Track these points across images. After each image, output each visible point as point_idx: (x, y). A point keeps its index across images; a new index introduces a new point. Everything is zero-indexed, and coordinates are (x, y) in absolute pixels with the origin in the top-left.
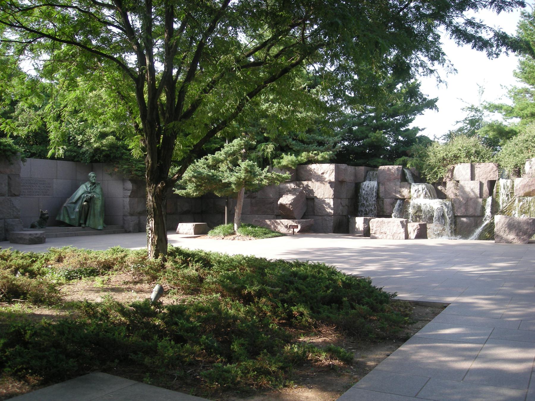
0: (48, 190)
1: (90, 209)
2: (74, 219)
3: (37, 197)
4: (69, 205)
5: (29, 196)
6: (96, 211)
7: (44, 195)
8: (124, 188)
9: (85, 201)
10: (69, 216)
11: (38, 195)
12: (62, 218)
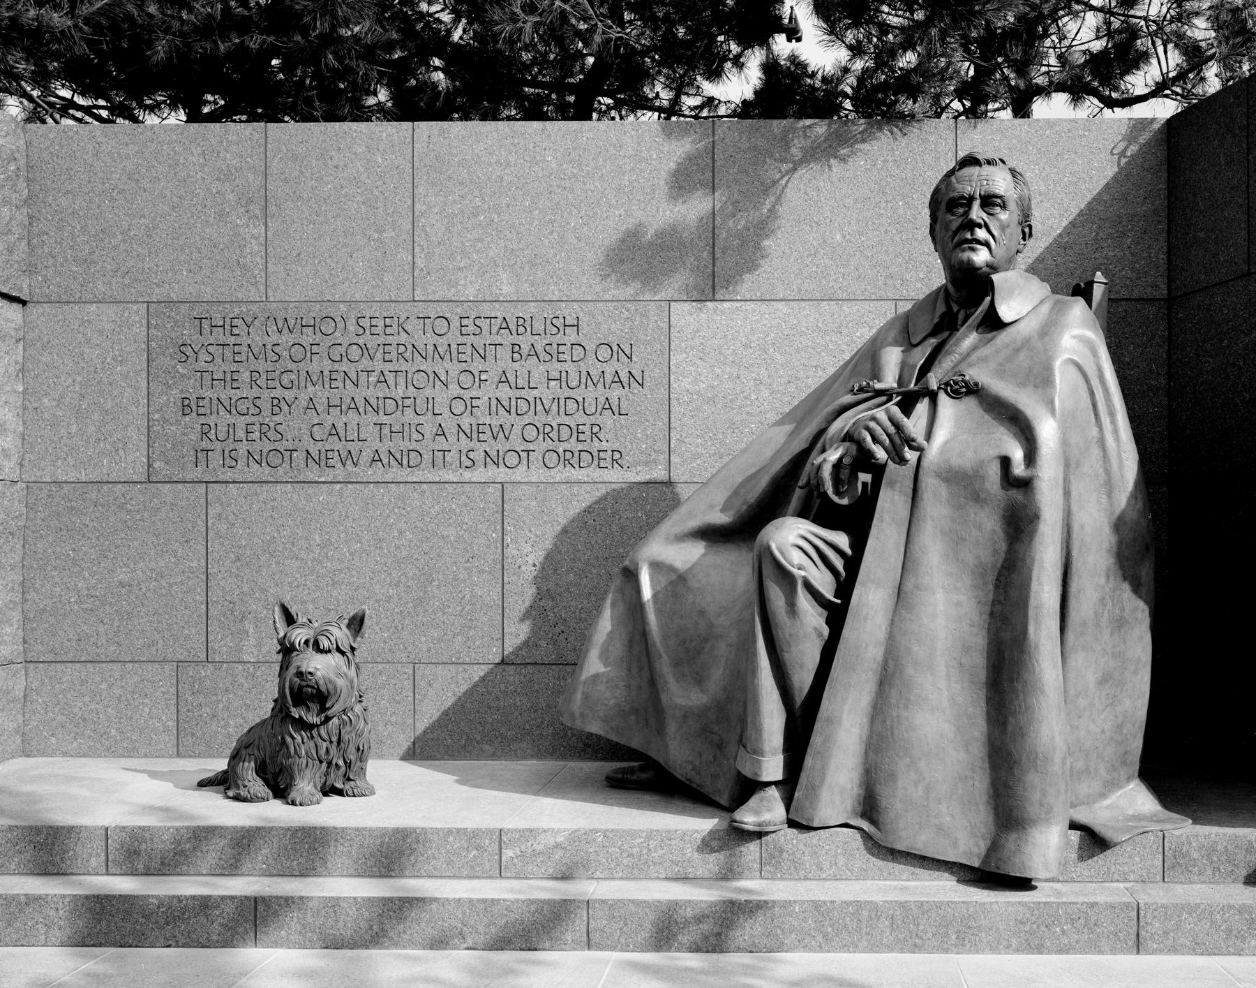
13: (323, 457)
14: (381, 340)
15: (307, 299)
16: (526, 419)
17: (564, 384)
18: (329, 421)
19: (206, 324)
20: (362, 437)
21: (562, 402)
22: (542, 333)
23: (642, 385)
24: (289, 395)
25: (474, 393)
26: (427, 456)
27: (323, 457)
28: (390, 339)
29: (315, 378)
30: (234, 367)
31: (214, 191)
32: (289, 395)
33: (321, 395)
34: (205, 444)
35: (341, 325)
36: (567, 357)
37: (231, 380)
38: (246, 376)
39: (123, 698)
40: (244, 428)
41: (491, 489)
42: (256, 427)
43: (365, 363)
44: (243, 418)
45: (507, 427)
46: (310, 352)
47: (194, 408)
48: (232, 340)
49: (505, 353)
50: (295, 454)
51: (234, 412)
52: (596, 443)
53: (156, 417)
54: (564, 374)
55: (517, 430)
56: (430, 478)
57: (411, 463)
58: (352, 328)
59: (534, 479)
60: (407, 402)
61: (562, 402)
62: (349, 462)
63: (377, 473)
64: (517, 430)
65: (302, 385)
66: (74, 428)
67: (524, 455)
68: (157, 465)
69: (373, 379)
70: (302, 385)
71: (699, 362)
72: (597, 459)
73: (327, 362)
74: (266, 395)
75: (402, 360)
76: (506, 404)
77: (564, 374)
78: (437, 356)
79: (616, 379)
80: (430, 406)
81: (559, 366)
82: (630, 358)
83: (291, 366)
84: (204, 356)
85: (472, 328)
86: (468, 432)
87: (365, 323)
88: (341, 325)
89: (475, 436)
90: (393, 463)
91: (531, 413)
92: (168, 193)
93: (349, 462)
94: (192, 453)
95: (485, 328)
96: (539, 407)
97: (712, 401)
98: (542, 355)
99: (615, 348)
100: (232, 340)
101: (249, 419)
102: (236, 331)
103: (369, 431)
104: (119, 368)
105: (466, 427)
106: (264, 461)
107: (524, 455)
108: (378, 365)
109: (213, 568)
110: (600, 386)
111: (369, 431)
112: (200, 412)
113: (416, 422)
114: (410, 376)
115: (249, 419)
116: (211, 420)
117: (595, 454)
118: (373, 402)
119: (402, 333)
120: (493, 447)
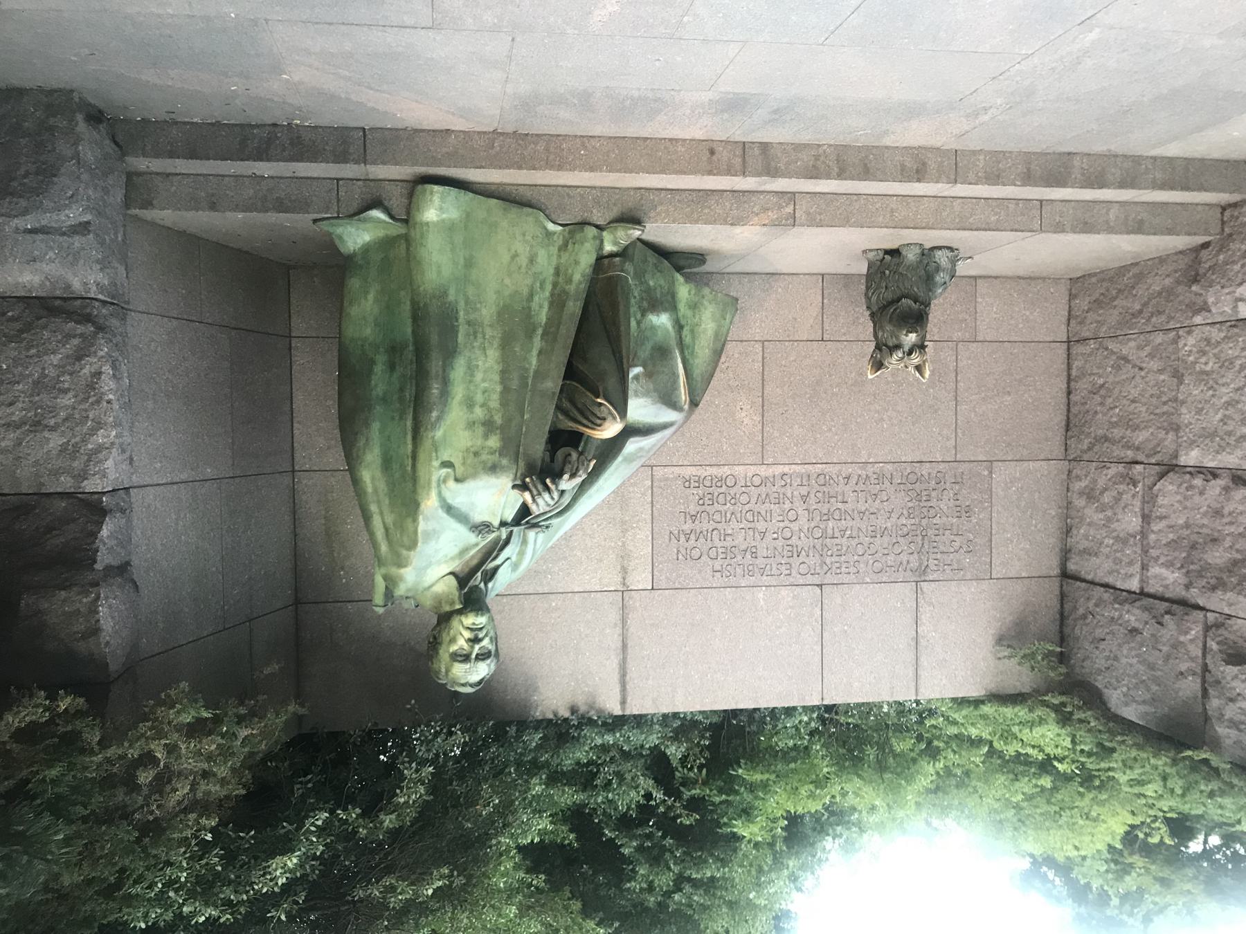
0: (694, 517)
3: (779, 470)
16: (747, 507)
25: (782, 524)
41: (771, 460)
49: (762, 552)
56: (810, 467)
59: (741, 468)
60: (825, 517)
63: (849, 469)
64: (753, 500)
69: (848, 532)
72: (700, 481)
89: (781, 496)
90: (834, 476)
96: (739, 515)
101: (929, 504)
103: (851, 497)
105: (787, 502)
110: (698, 531)
111: (851, 497)
115: (929, 504)
118: (848, 518)
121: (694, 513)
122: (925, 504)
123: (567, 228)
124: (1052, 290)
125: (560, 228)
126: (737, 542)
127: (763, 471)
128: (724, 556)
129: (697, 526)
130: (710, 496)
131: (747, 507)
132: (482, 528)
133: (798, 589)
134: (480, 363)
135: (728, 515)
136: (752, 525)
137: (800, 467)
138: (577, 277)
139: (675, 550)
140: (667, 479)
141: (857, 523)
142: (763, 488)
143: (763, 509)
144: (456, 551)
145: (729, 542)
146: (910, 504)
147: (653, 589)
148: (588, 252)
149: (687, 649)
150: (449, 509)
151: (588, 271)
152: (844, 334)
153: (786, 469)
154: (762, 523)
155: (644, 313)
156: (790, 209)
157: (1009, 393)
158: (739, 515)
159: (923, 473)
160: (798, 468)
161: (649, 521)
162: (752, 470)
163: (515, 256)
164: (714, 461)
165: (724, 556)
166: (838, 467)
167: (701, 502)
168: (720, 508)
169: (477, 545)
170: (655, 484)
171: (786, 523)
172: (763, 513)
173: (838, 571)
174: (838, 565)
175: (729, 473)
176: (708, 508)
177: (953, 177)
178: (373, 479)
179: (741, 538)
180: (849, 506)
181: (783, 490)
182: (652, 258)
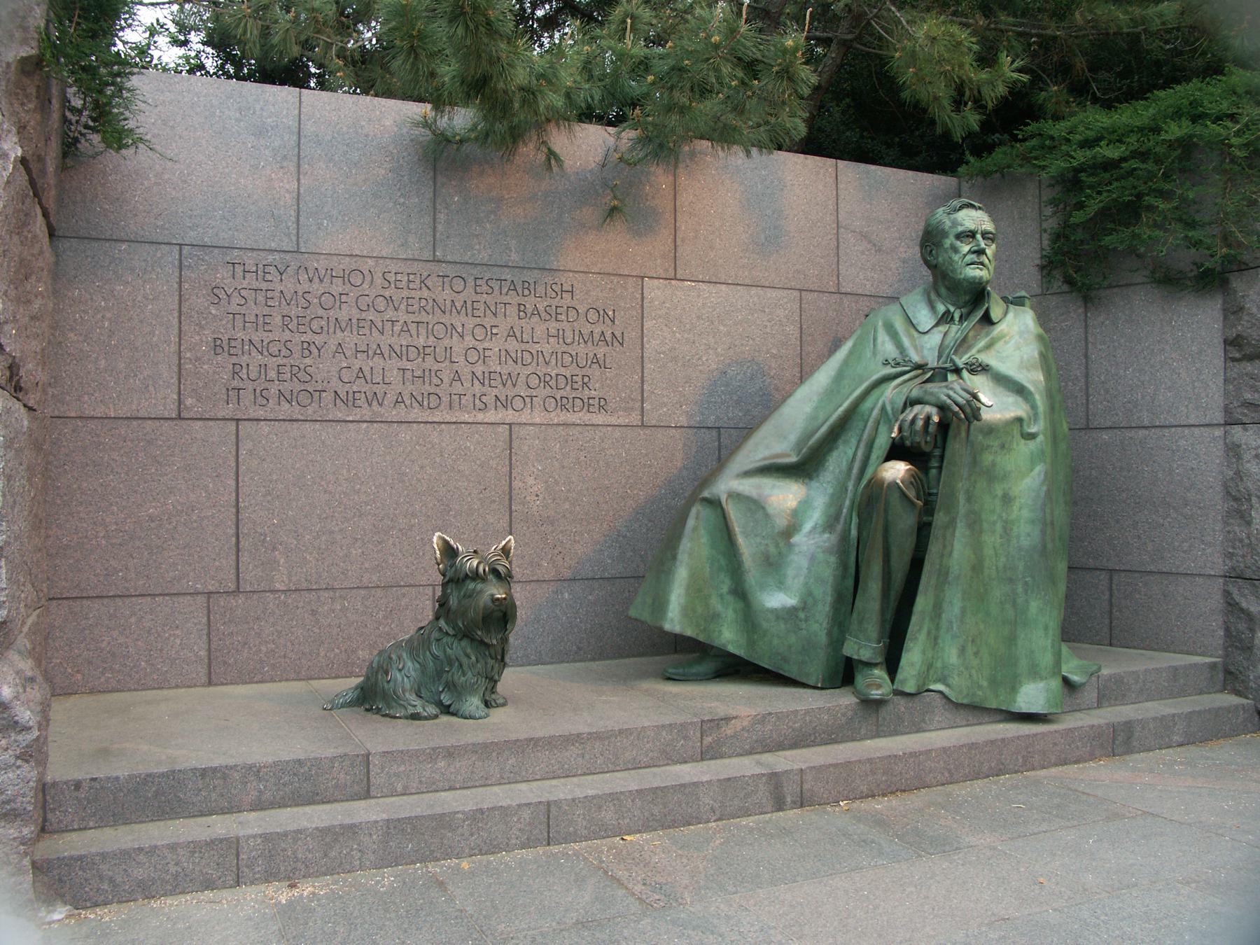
1: (940, 518)
2: (789, 614)
3: (491, 416)
4: (747, 486)
5: (416, 414)
6: (991, 540)
7: (562, 404)
8: (1233, 343)
9: (896, 451)
10: (741, 593)
11: (505, 404)
12: (675, 620)
13: (350, 398)
14: (405, 293)
15: (337, 252)
16: (530, 370)
17: (561, 340)
18: (357, 364)
19: (239, 269)
20: (387, 380)
21: (559, 356)
22: (543, 295)
23: (622, 344)
24: (319, 340)
25: (486, 345)
26: (445, 399)
27: (350, 398)
28: (413, 293)
29: (343, 325)
30: (266, 311)
31: (250, 145)
32: (319, 340)
33: (350, 339)
34: (235, 383)
35: (368, 278)
36: (563, 317)
37: (262, 323)
38: (278, 320)
39: (153, 631)
40: (276, 369)
41: (500, 429)
42: (288, 369)
43: (390, 314)
44: (275, 359)
45: (514, 375)
46: (339, 300)
47: (226, 349)
48: (264, 286)
49: (511, 310)
50: (324, 394)
51: (266, 353)
52: (586, 391)
53: (188, 355)
54: (561, 332)
55: (522, 378)
56: (448, 419)
57: (431, 405)
58: (379, 281)
59: (538, 420)
60: (428, 350)
61: (559, 356)
62: (375, 403)
63: (400, 413)
64: (522, 378)
65: (331, 330)
66: (103, 363)
67: (528, 400)
68: (189, 402)
69: (397, 328)
70: (331, 330)
71: (665, 328)
72: (587, 405)
73: (355, 311)
74: (298, 338)
75: (423, 313)
76: (514, 355)
77: (561, 332)
78: (454, 310)
79: (602, 338)
80: (448, 356)
81: (557, 325)
82: (613, 321)
83: (320, 312)
84: (236, 300)
85: (485, 288)
86: (481, 378)
87: (391, 277)
88: (368, 278)
89: (487, 382)
90: (415, 404)
91: (534, 364)
92: (204, 142)
93: (375, 403)
94: (224, 391)
95: (497, 288)
96: (541, 359)
97: (675, 359)
98: (543, 314)
99: (602, 312)
100: (264, 286)
101: (280, 361)
102: (268, 277)
103: (394, 376)
104: (150, 307)
105: (479, 374)
106: (294, 400)
107: (528, 400)
108: (402, 316)
109: (244, 501)
110: (590, 343)
111: (394, 376)
112: (232, 352)
113: (436, 368)
114: (430, 326)
115: (280, 361)
116: (244, 360)
117: (586, 401)
118: (397, 348)
119: (424, 288)
120: (502, 393)
121: (594, 366)
122: (285, 361)
123: (926, 688)
124: (79, 677)
125: (932, 687)
126: (543, 327)
127: (510, 416)
128: (559, 310)
129: (591, 351)
130: (575, 386)
131: (530, 370)
132: (978, 368)
133: (466, 259)
134: (999, 541)
135: (553, 362)
136: (524, 346)
137: (462, 419)
138: (922, 636)
139: (616, 322)
140: (625, 410)
141: (385, 341)
142: (511, 394)
143: (510, 367)
144: (998, 346)
145: (553, 326)
146: (308, 361)
147: (643, 278)
148: (913, 664)
149: (604, 201)
150: (1020, 390)
151: (908, 644)
152: (404, 595)
153: (480, 417)
154: (510, 348)
155: (804, 606)
156: (708, 740)
157: (151, 519)
158: (541, 359)
159: (287, 405)
160: (466, 418)
161: (646, 360)
162: (524, 417)
163: (976, 654)
164: (572, 431)
165: (559, 310)
166: (411, 417)
167: (586, 380)
168: (563, 371)
169: (979, 351)
170: (639, 404)
171: (480, 347)
172: (510, 362)
173: (412, 277)
174: (411, 286)
175: (553, 414)
176: (578, 371)
177: (553, 809)
178: (1062, 426)
179: (538, 333)
180: (395, 363)
181: (484, 390)
182: (791, 671)
